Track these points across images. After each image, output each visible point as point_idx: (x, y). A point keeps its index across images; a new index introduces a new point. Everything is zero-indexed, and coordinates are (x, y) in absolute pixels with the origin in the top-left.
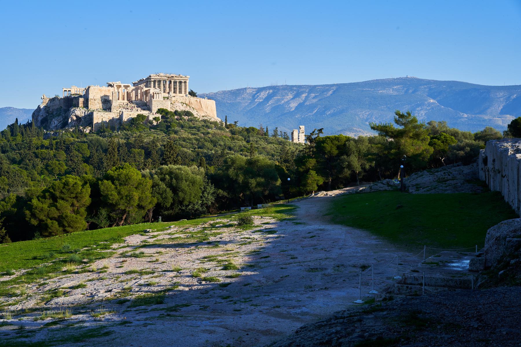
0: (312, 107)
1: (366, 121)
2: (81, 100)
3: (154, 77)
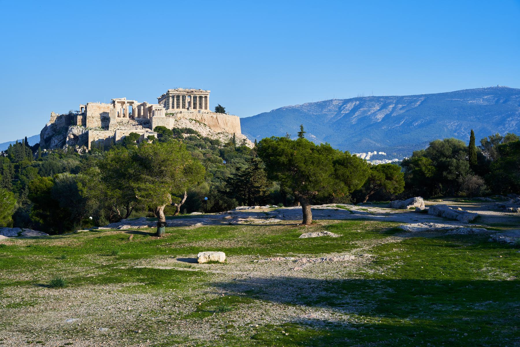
0: (399, 118)
1: (455, 132)
2: (79, 118)
3: (172, 92)
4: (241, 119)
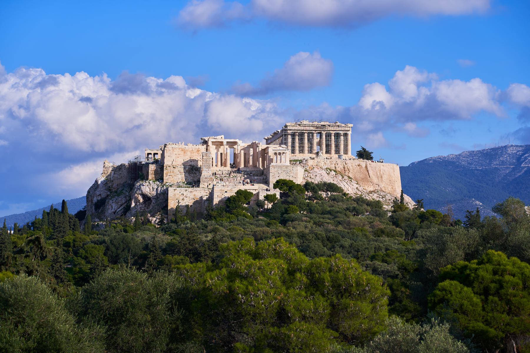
3: (292, 127)
4: (401, 168)
